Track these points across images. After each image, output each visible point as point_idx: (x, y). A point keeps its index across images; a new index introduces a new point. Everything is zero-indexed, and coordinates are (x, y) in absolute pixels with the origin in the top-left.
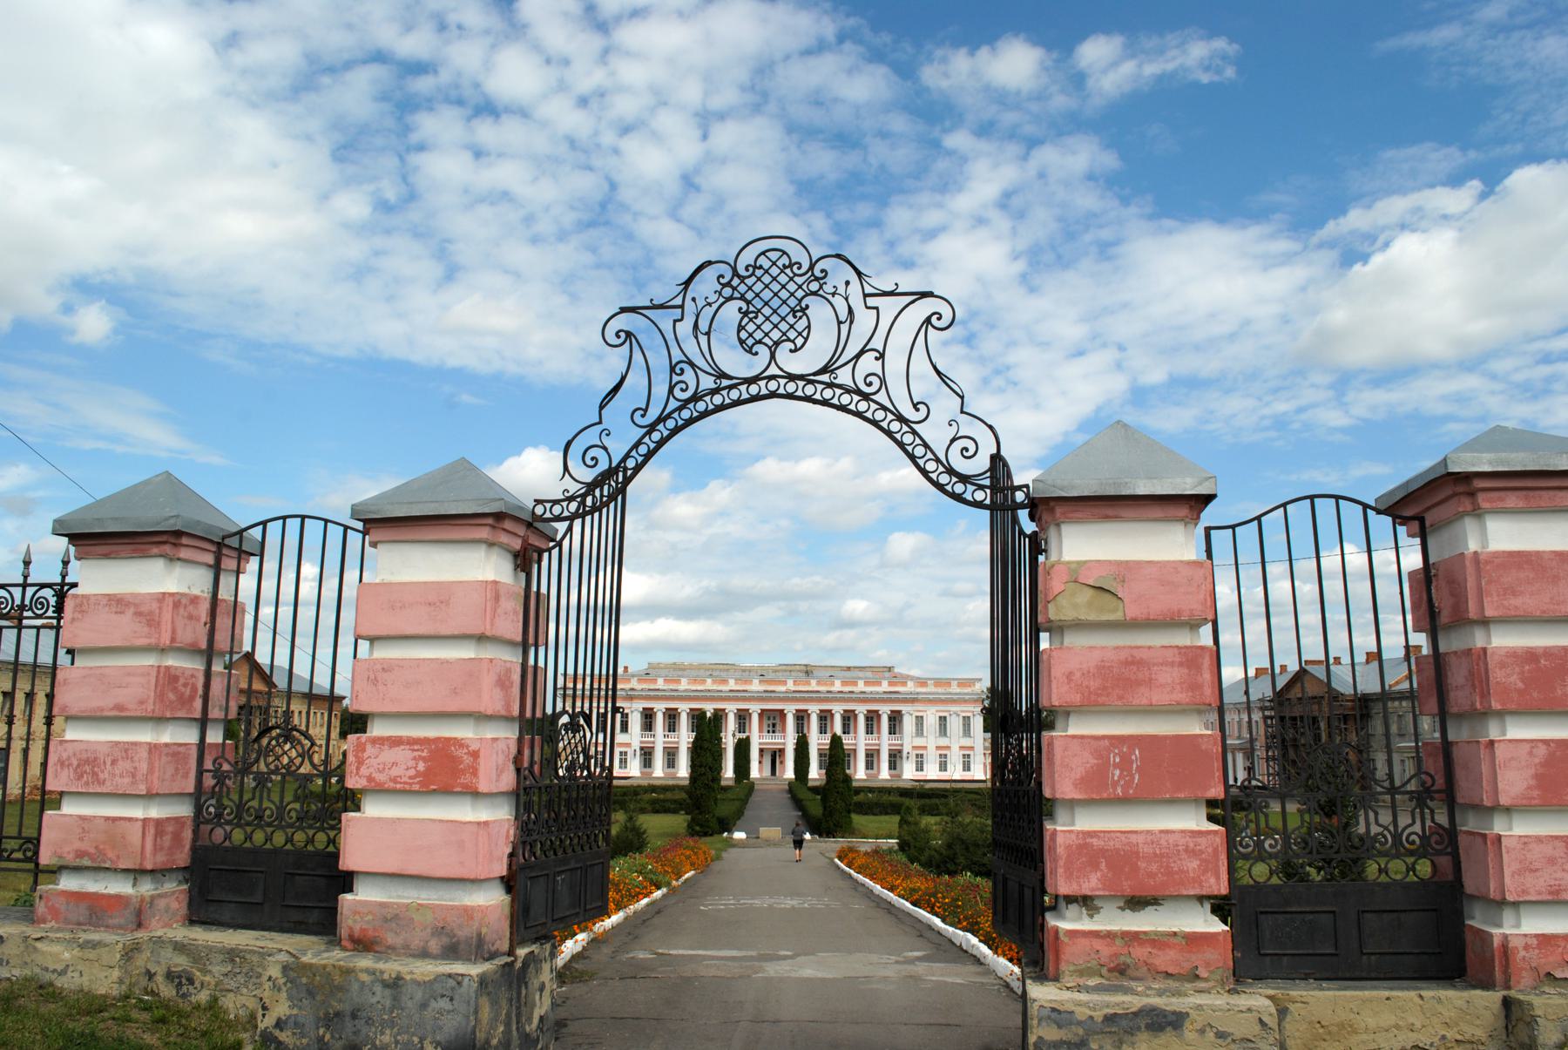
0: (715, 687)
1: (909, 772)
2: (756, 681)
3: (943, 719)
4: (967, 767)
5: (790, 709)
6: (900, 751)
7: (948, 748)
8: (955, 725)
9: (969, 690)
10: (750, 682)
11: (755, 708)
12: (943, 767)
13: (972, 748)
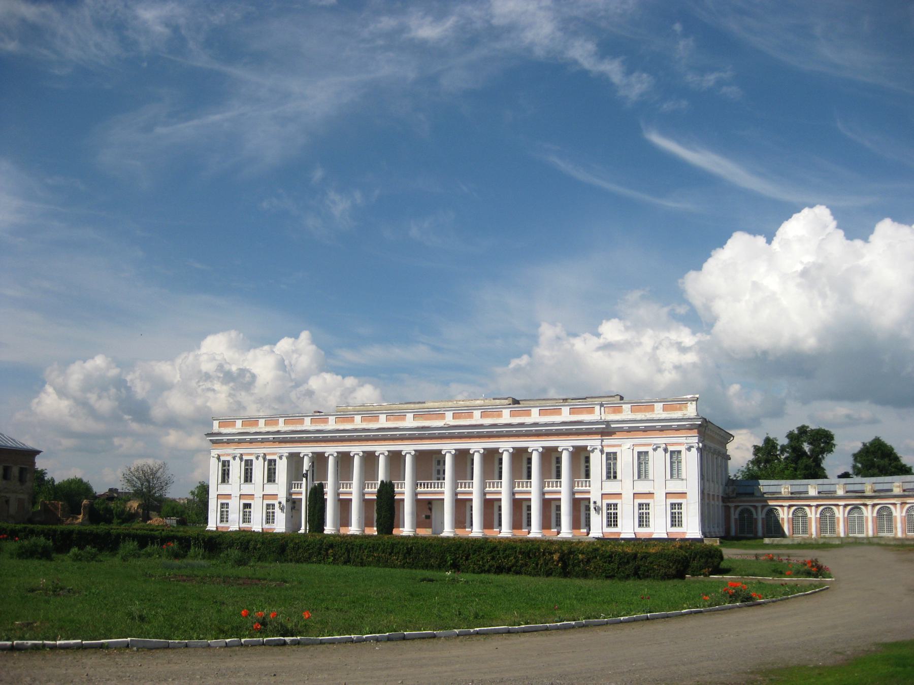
0: (365, 425)
1: (598, 528)
2: (410, 416)
3: (643, 456)
4: (676, 520)
5: (448, 448)
6: (589, 499)
7: (650, 494)
8: (658, 462)
9: (677, 414)
10: (402, 417)
11: (408, 449)
12: (643, 520)
13: (683, 494)
